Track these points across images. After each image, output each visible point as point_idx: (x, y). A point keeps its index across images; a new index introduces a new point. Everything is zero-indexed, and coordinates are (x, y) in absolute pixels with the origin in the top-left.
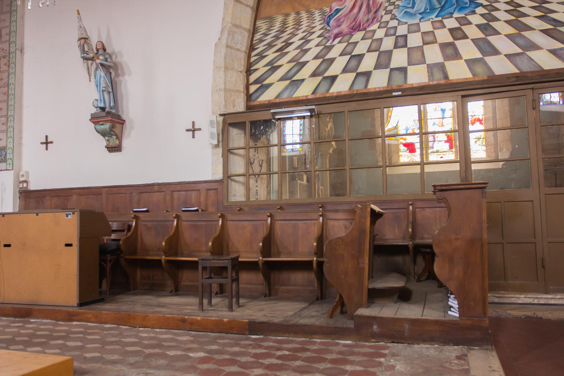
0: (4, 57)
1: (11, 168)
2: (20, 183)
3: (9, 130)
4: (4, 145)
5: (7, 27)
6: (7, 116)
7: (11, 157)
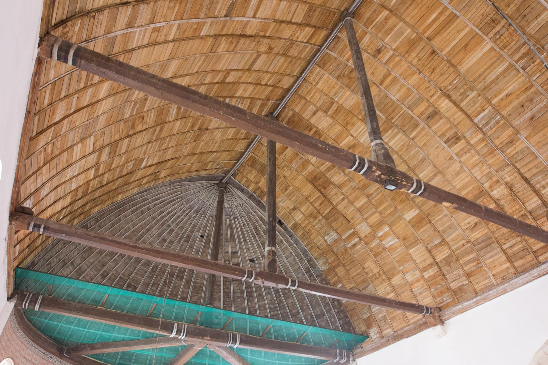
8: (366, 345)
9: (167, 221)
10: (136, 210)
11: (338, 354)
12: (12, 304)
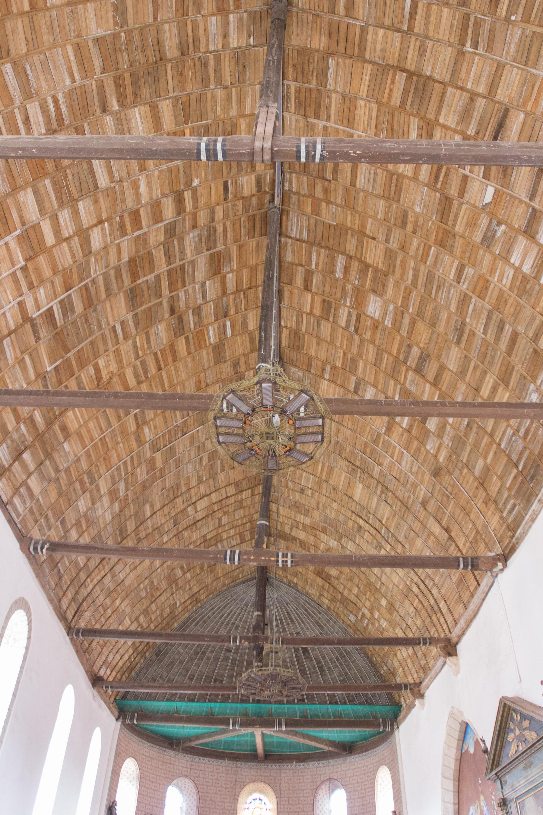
8: (403, 713)
9: (230, 620)
10: (198, 622)
11: (381, 724)
12: (119, 723)
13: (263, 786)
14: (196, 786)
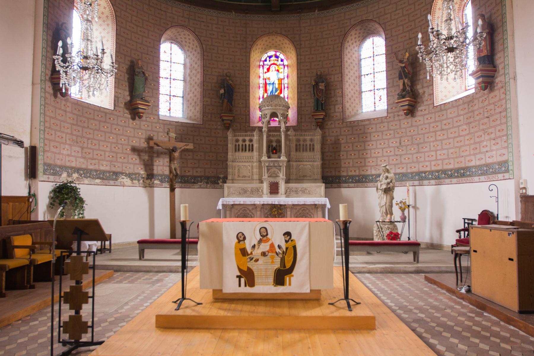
0: (502, 87)
1: (512, 178)
2: (521, 189)
3: (509, 147)
4: (507, 159)
5: (502, 62)
6: (507, 135)
7: (512, 168)
13: (279, 39)
14: (198, 38)
